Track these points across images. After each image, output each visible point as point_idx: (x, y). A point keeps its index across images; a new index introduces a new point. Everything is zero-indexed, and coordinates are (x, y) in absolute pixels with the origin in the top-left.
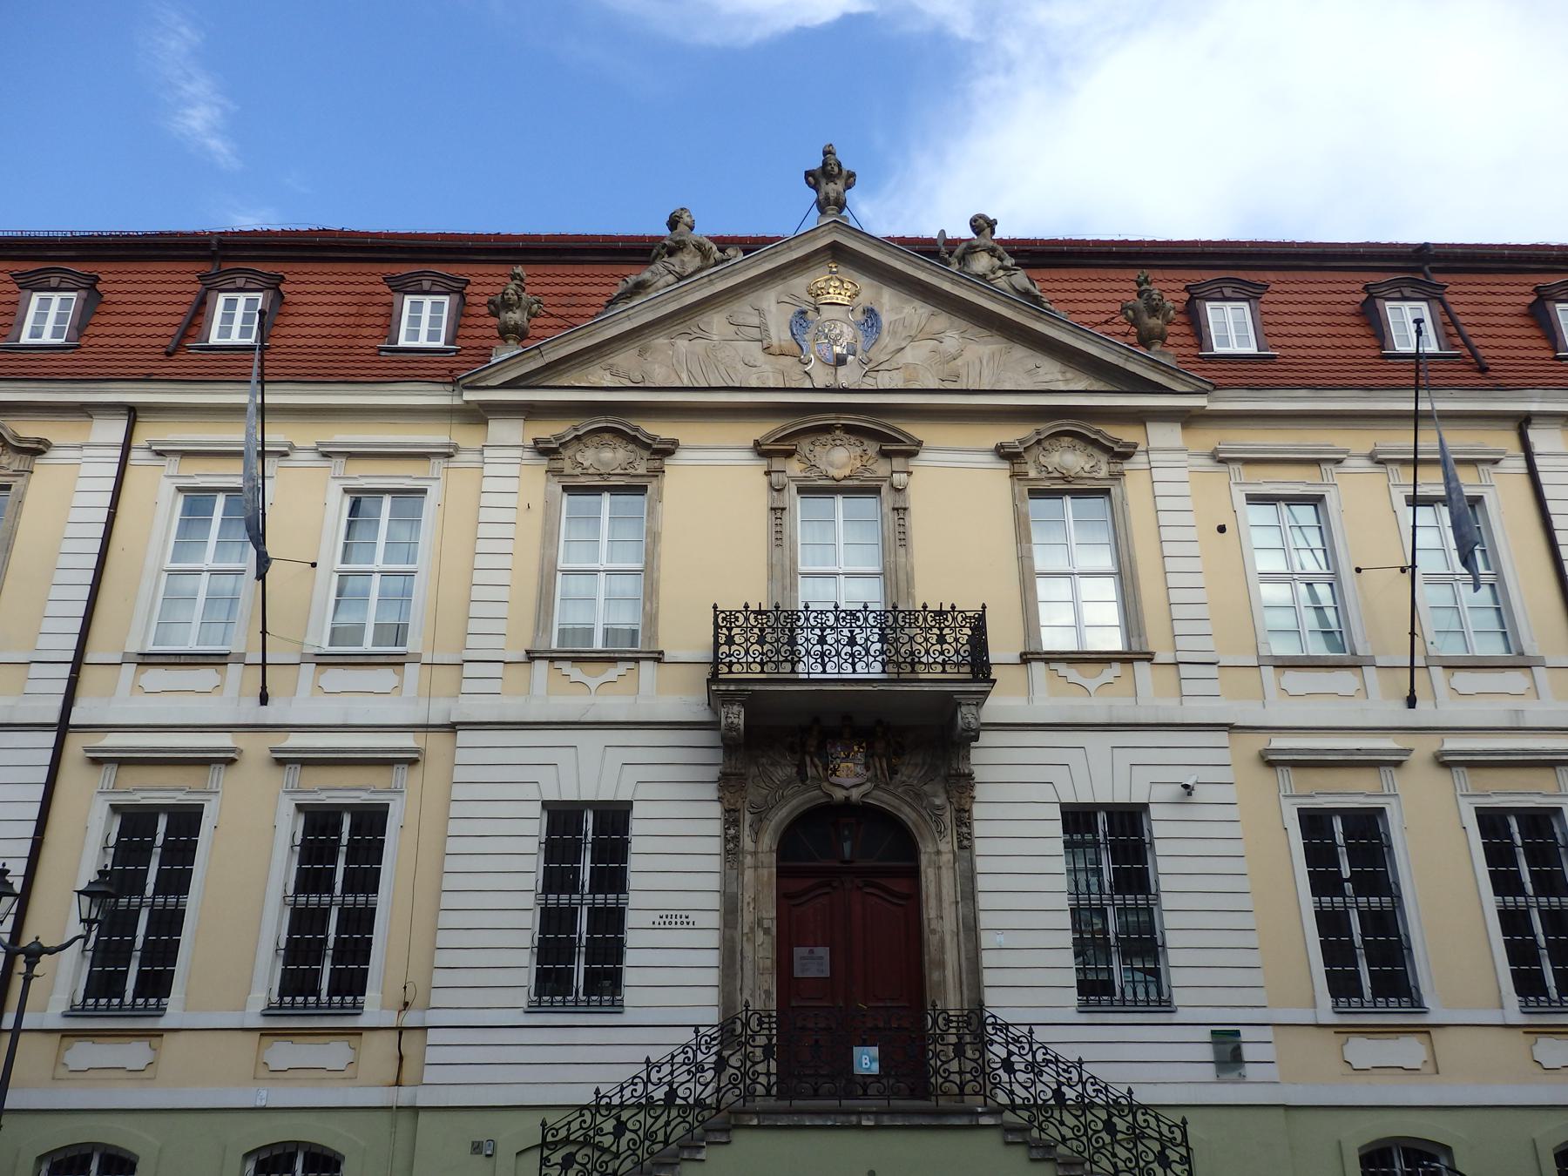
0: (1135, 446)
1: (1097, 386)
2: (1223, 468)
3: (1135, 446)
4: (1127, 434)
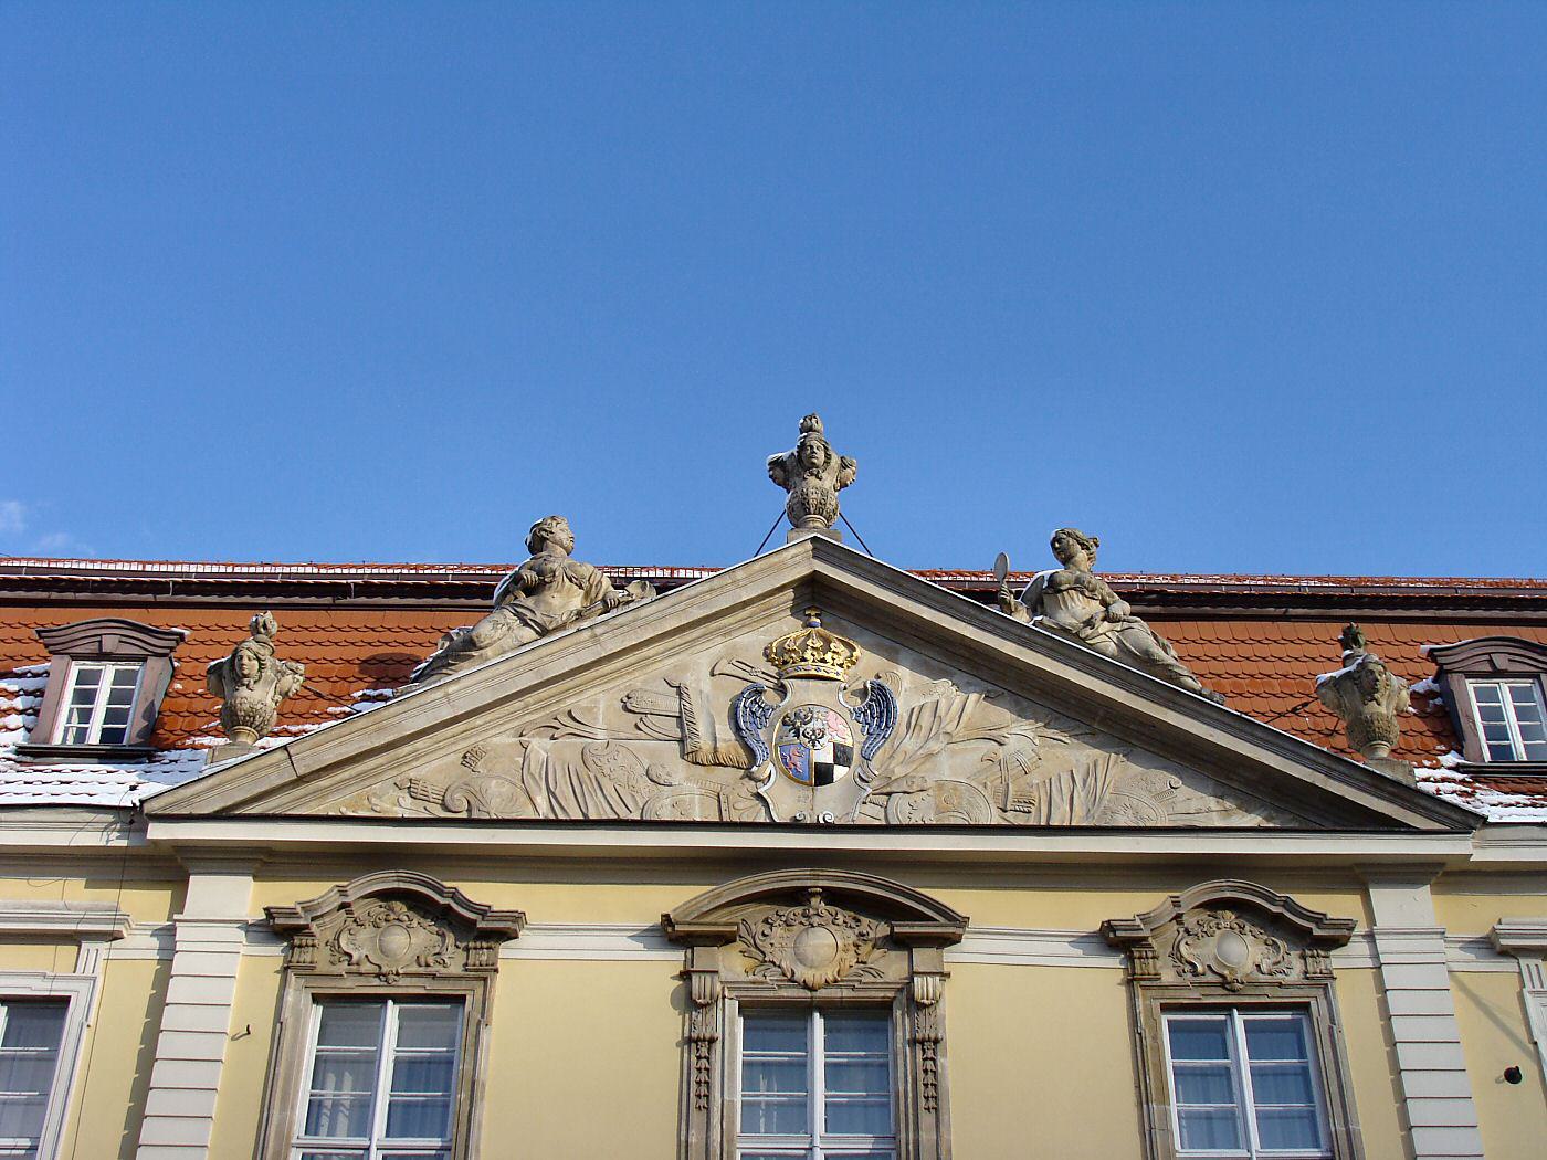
0: (1349, 926)
1: (1253, 820)
2: (1509, 965)
3: (1349, 926)
4: (1338, 905)
